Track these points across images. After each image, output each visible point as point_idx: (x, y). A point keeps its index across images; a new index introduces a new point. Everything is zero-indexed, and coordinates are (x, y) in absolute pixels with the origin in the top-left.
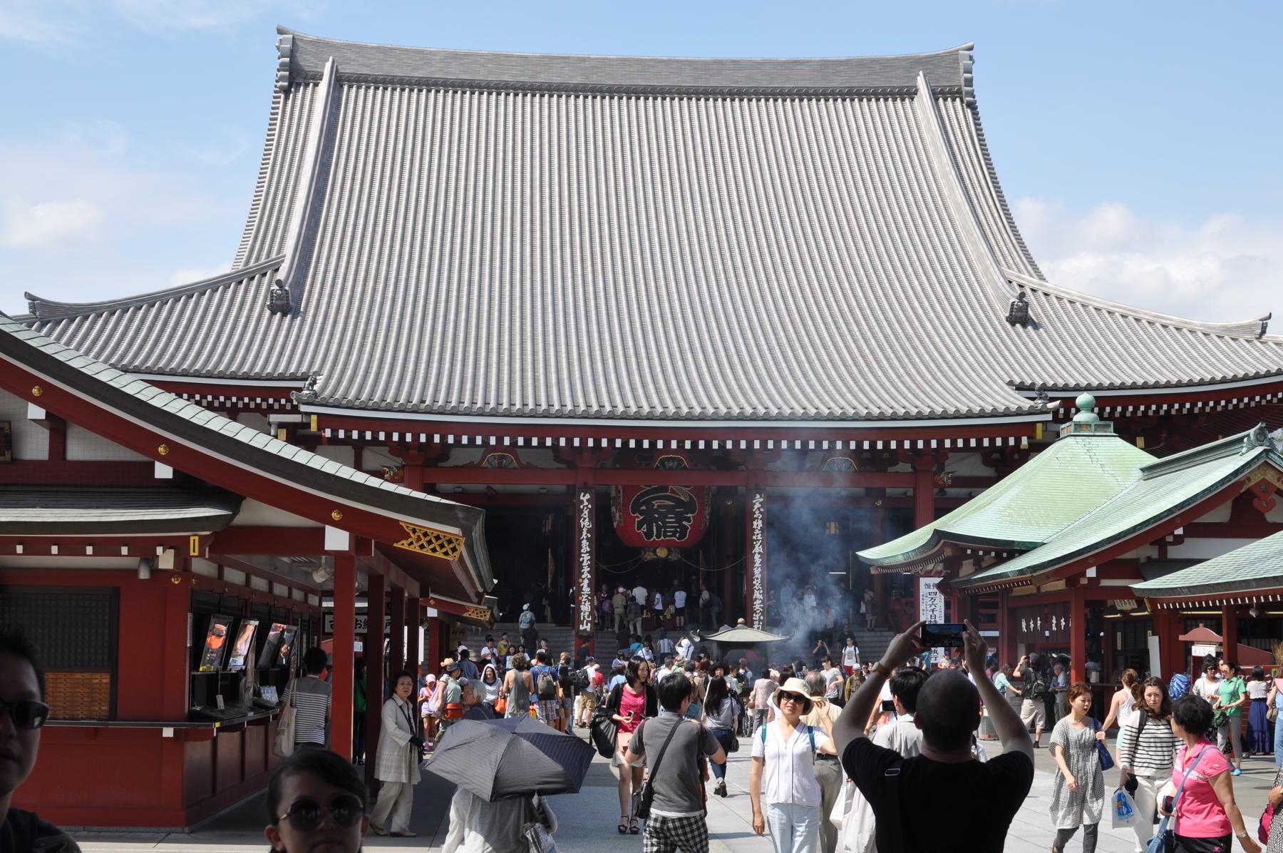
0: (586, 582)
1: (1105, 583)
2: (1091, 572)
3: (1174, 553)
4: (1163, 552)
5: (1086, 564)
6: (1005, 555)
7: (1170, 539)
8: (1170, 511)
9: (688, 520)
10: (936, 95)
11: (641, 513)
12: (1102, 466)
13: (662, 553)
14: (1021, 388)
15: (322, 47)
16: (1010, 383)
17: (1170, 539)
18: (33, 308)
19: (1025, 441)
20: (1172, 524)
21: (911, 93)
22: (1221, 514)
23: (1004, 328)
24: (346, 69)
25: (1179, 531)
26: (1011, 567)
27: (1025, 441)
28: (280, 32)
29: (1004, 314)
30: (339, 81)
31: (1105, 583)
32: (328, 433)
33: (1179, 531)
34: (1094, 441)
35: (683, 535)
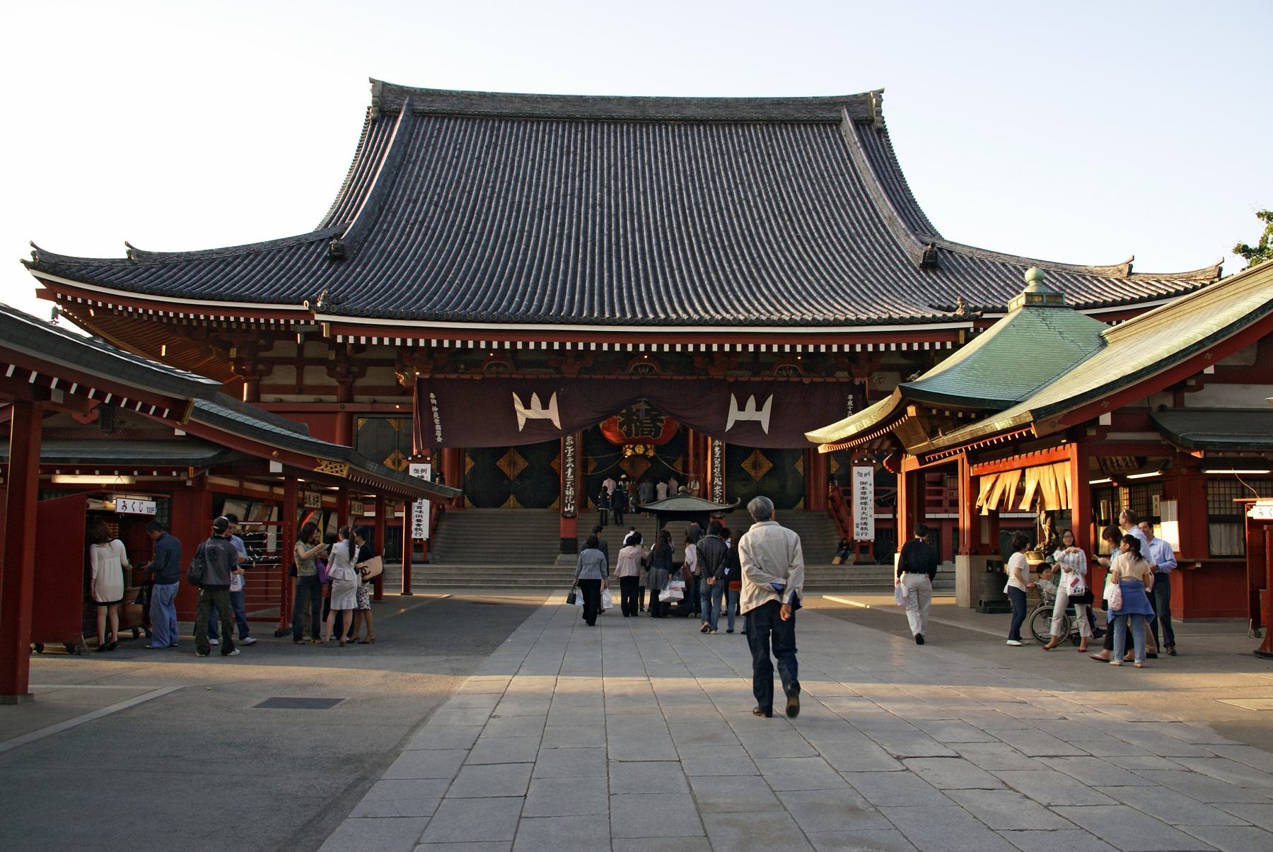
0: (570, 471)
1: (1111, 436)
2: (1106, 419)
3: (1192, 400)
4: (1179, 402)
5: (1099, 409)
6: (973, 416)
7: (1192, 383)
8: (1200, 344)
9: (661, 421)
10: (858, 124)
11: (622, 415)
12: (1060, 333)
13: (640, 450)
14: (940, 308)
15: (403, 91)
16: (931, 306)
17: (1192, 383)
18: (129, 253)
19: (949, 345)
20: (1201, 361)
21: (838, 122)
22: (1244, 358)
23: (918, 273)
24: (420, 107)
25: (1210, 370)
26: (1000, 422)
27: (949, 345)
28: (372, 81)
30: (416, 115)
31: (1111, 436)
32: (340, 339)
33: (1210, 370)
34: (1048, 312)
35: (657, 434)
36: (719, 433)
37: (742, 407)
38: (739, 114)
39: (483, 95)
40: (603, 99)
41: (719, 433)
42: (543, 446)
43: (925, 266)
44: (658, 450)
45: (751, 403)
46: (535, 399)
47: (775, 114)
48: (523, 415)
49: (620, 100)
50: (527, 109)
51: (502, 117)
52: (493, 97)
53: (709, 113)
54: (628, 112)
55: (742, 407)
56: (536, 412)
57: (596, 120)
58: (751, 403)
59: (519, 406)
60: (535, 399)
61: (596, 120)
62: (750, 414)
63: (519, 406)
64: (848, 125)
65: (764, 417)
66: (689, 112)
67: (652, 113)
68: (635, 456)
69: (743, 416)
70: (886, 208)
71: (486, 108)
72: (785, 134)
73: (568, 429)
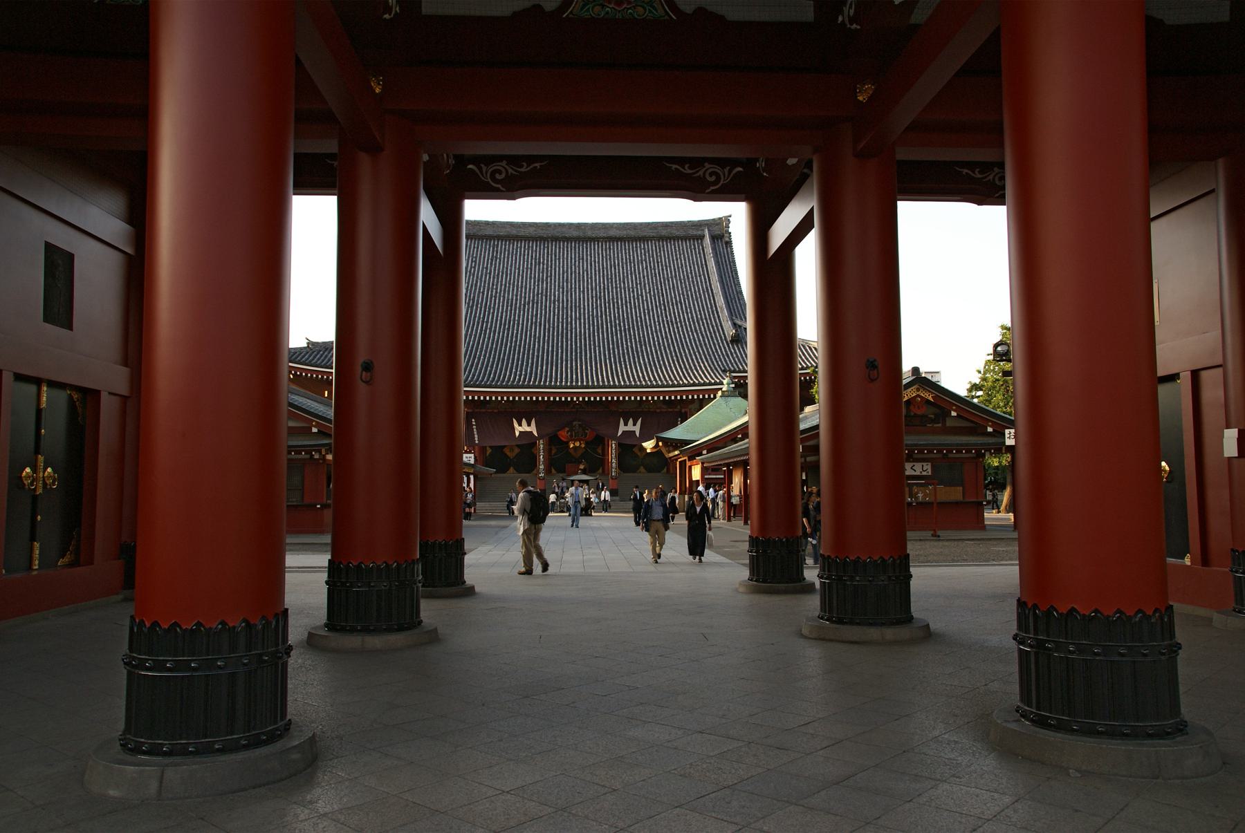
10: (714, 238)
13: (577, 444)
21: (702, 237)
29: (729, 339)
36: (614, 437)
37: (626, 424)
38: (642, 234)
39: (487, 223)
40: (560, 225)
41: (614, 437)
42: (528, 442)
43: (732, 341)
44: (587, 443)
45: (631, 421)
46: (524, 422)
47: (664, 233)
48: (518, 429)
49: (571, 225)
50: (514, 232)
51: (499, 238)
52: (494, 224)
53: (623, 233)
54: (575, 234)
55: (626, 424)
56: (525, 427)
57: (556, 239)
58: (631, 421)
59: (516, 425)
60: (524, 422)
61: (556, 239)
62: (630, 427)
63: (516, 425)
64: (707, 240)
65: (637, 429)
66: (612, 233)
67: (589, 234)
68: (575, 448)
69: (626, 429)
70: (721, 301)
71: (489, 232)
72: (669, 247)
73: (541, 436)
